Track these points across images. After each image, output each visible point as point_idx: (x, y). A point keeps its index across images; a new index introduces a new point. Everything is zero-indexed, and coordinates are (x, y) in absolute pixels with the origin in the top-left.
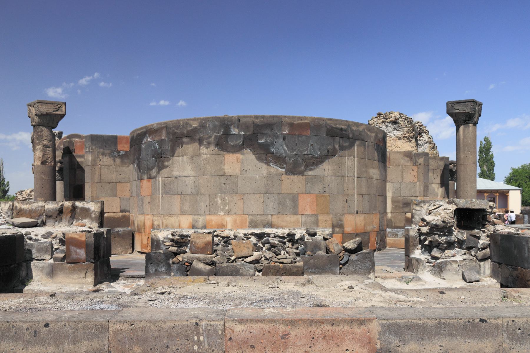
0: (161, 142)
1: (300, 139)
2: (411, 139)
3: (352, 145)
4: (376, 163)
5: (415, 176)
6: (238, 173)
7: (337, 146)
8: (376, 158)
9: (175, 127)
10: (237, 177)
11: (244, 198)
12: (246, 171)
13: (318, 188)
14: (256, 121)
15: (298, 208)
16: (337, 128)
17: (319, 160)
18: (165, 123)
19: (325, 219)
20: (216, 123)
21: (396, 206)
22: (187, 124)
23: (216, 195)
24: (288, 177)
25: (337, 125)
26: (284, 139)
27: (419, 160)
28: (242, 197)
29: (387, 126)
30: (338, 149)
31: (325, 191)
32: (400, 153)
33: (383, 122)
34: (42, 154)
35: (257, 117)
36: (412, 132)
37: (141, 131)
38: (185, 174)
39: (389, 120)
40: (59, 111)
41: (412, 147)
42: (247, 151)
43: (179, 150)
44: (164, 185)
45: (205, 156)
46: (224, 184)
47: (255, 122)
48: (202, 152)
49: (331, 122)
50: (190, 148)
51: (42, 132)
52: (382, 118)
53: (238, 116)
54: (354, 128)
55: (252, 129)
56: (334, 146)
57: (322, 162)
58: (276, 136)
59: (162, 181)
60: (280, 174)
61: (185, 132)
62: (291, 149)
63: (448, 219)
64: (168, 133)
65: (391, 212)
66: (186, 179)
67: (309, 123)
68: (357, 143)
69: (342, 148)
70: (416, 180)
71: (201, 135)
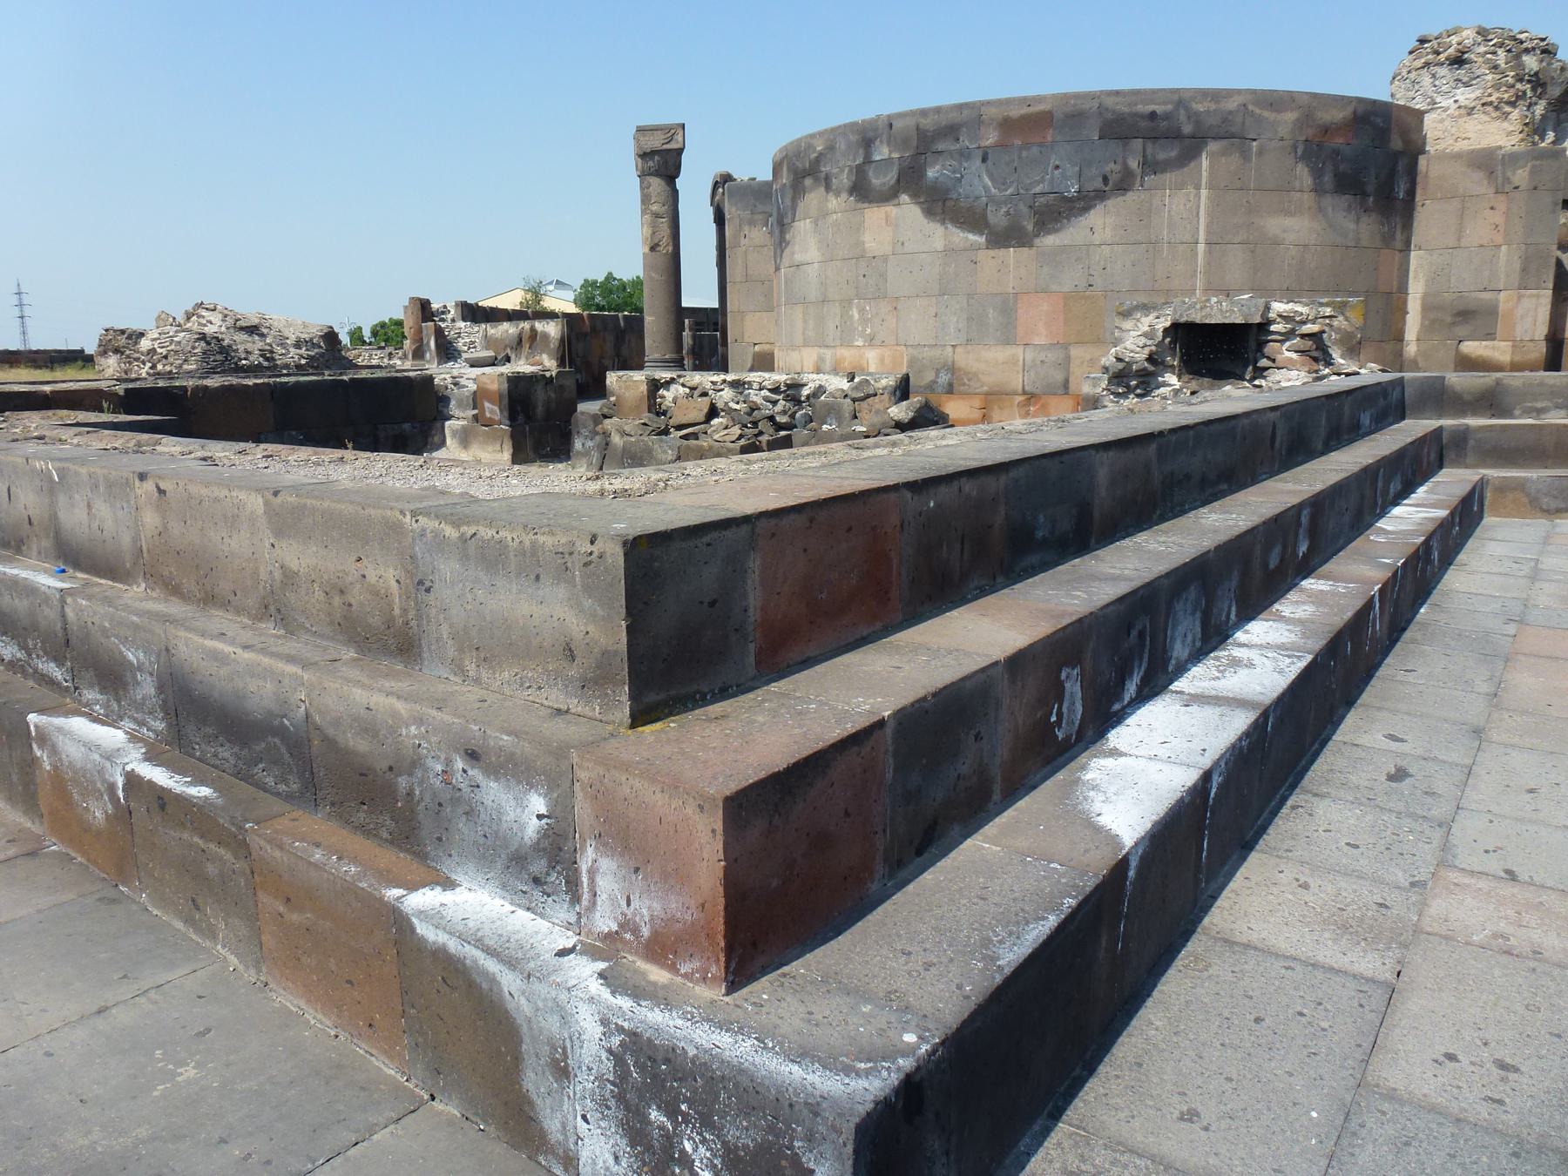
1: (1024, 154)
2: (1507, 109)
4: (1308, 198)
5: (1497, 226)
6: (888, 249)
7: (1133, 164)
10: (885, 258)
11: (899, 307)
12: (903, 244)
13: (1070, 279)
15: (1015, 327)
16: (1135, 115)
17: (1083, 202)
19: (1088, 357)
21: (1433, 322)
23: (850, 301)
24: (991, 253)
25: (1136, 105)
26: (984, 160)
27: (1514, 174)
29: (1434, 76)
30: (1139, 171)
31: (1090, 285)
32: (1457, 156)
33: (1427, 65)
34: (650, 232)
35: (924, 113)
36: (1513, 86)
39: (1442, 57)
40: (673, 142)
41: (1509, 134)
42: (905, 198)
47: (921, 126)
49: (1117, 99)
52: (1428, 54)
54: (1201, 108)
57: (1086, 209)
58: (965, 154)
60: (975, 248)
62: (1001, 183)
63: (1132, 351)
65: (1418, 340)
69: (1152, 167)
70: (1499, 239)
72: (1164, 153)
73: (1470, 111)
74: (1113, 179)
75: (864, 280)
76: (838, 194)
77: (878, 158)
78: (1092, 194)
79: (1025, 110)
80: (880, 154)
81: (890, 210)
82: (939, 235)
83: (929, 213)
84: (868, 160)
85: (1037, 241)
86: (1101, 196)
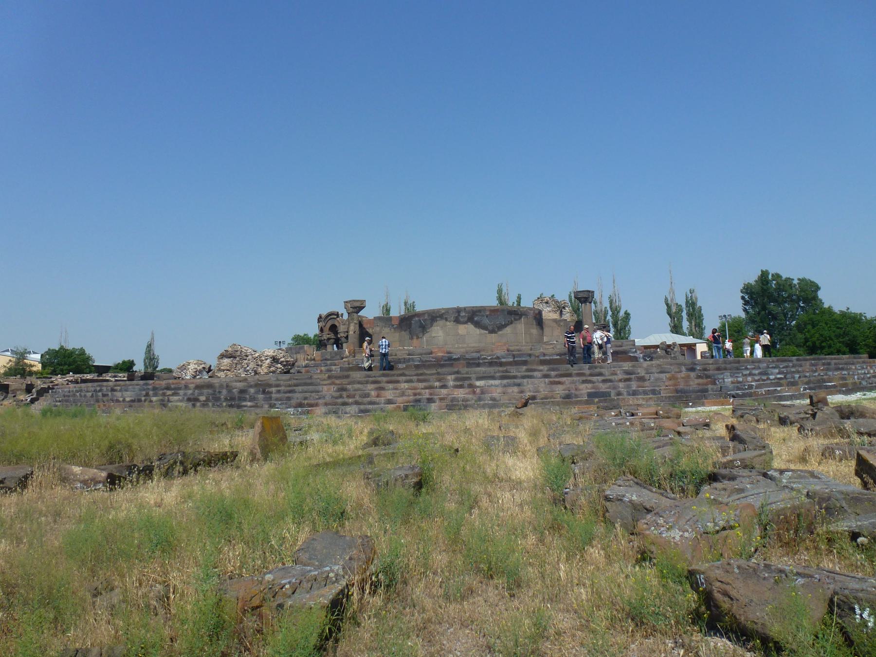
0: (425, 320)
3: (520, 318)
4: (535, 326)
7: (513, 319)
8: (535, 323)
10: (465, 335)
17: (505, 326)
35: (473, 307)
43: (435, 324)
44: (427, 341)
50: (441, 322)
54: (521, 310)
58: (483, 316)
64: (429, 316)
68: (523, 316)
69: (516, 320)
72: (517, 317)
73: (550, 312)
76: (450, 322)
81: (466, 326)
82: (478, 331)
83: (476, 326)
84: (459, 315)
86: (508, 325)
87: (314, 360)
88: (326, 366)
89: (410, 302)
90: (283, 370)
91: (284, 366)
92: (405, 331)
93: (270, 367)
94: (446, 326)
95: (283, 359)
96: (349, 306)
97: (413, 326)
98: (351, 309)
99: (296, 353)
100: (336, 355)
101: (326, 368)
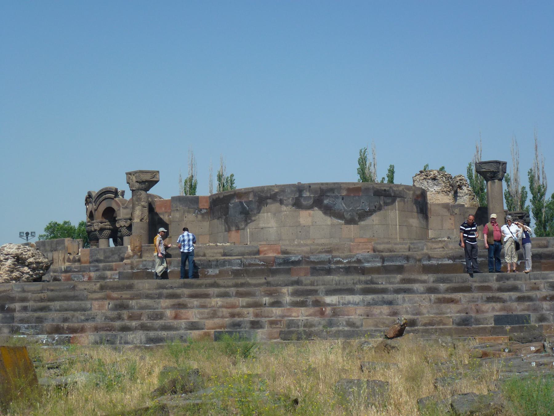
0: (249, 203)
1: (354, 198)
2: (449, 193)
3: (393, 201)
4: (415, 214)
7: (382, 203)
8: (415, 210)
9: (260, 192)
10: (309, 227)
12: (316, 222)
14: (322, 187)
16: (381, 190)
17: (370, 213)
18: (252, 188)
20: (293, 189)
22: (270, 190)
26: (343, 199)
27: (455, 210)
28: (313, 241)
29: (428, 182)
32: (439, 205)
33: (425, 179)
34: (141, 213)
35: (322, 184)
36: (449, 187)
37: (229, 194)
38: (269, 225)
39: (429, 177)
41: (450, 199)
42: (316, 208)
43: (264, 208)
44: (252, 234)
45: (285, 213)
46: (300, 232)
48: (283, 209)
49: (377, 185)
50: (273, 207)
51: (140, 195)
52: (424, 176)
53: (309, 184)
54: (395, 189)
55: (319, 192)
56: (380, 203)
57: (371, 215)
58: (336, 197)
59: (250, 232)
61: (269, 195)
64: (255, 196)
66: (271, 229)
67: (360, 187)
68: (398, 199)
69: (386, 204)
70: (453, 227)
71: (281, 197)
72: (389, 201)
73: (439, 193)
74: (377, 206)
75: (300, 233)
76: (287, 205)
77: (305, 196)
78: (372, 211)
79: (354, 186)
80: (306, 194)
81: (311, 212)
82: (329, 220)
83: (325, 213)
84: (301, 196)
85: (359, 223)
86: (374, 211)
87: (79, 261)
88: (97, 270)
89: (227, 174)
90: (32, 276)
91: (34, 270)
92: (218, 218)
93: (12, 272)
94: (281, 212)
95: (31, 260)
96: (134, 179)
97: (231, 211)
98: (137, 185)
99: (52, 251)
100: (113, 254)
101: (98, 273)
